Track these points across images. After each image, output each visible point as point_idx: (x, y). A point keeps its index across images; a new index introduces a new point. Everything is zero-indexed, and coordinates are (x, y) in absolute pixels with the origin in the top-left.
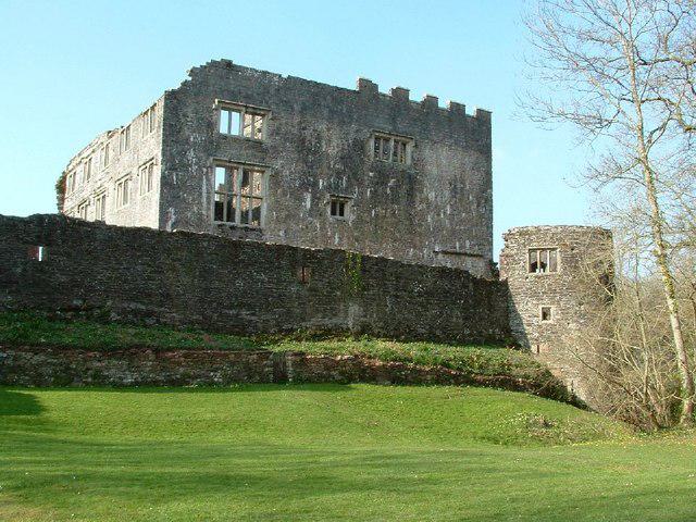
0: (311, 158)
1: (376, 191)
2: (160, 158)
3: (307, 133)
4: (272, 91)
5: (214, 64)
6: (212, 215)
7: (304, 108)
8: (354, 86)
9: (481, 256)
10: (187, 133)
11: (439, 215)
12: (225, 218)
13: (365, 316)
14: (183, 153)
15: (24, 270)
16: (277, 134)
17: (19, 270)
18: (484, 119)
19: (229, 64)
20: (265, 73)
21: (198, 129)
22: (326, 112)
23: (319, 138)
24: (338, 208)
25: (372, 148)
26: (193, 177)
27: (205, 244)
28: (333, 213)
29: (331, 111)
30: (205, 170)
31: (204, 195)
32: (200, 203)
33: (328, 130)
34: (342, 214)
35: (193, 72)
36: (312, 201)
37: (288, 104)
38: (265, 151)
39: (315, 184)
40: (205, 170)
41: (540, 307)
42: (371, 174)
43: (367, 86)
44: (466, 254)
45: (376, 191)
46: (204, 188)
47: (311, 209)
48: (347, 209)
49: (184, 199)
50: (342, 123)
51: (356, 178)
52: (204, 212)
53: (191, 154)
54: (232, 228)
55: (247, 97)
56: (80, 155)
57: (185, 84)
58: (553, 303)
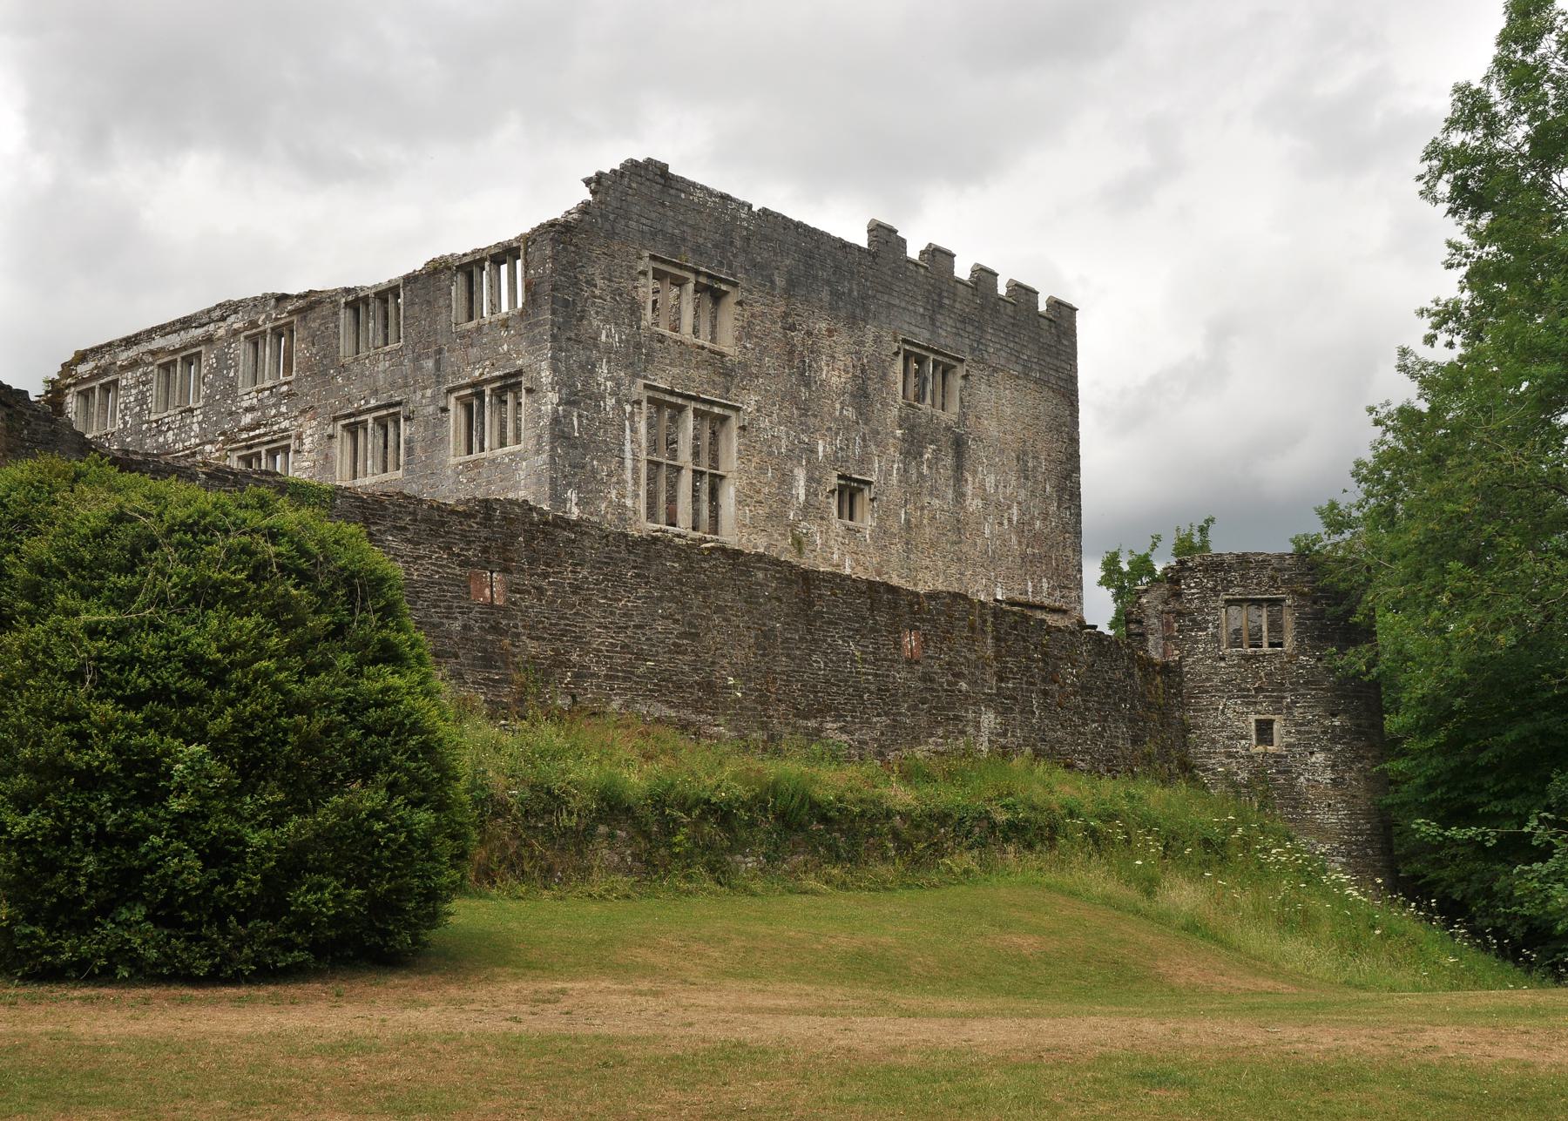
2: (546, 377)
6: (642, 507)
7: (792, 284)
8: (862, 240)
9: (1065, 612)
11: (1001, 524)
12: (663, 518)
13: (1004, 735)
14: (589, 368)
15: (465, 627)
16: (749, 336)
17: (457, 626)
18: (1063, 315)
19: (663, 168)
20: (725, 198)
21: (613, 318)
22: (825, 295)
24: (850, 492)
25: (900, 377)
30: (628, 408)
31: (629, 463)
33: (830, 332)
36: (810, 479)
37: (761, 270)
38: (728, 374)
39: (813, 451)
40: (628, 408)
41: (1252, 718)
43: (884, 236)
46: (628, 447)
49: (594, 471)
50: (853, 321)
52: (629, 503)
53: (603, 370)
57: (584, 209)
58: (1277, 711)
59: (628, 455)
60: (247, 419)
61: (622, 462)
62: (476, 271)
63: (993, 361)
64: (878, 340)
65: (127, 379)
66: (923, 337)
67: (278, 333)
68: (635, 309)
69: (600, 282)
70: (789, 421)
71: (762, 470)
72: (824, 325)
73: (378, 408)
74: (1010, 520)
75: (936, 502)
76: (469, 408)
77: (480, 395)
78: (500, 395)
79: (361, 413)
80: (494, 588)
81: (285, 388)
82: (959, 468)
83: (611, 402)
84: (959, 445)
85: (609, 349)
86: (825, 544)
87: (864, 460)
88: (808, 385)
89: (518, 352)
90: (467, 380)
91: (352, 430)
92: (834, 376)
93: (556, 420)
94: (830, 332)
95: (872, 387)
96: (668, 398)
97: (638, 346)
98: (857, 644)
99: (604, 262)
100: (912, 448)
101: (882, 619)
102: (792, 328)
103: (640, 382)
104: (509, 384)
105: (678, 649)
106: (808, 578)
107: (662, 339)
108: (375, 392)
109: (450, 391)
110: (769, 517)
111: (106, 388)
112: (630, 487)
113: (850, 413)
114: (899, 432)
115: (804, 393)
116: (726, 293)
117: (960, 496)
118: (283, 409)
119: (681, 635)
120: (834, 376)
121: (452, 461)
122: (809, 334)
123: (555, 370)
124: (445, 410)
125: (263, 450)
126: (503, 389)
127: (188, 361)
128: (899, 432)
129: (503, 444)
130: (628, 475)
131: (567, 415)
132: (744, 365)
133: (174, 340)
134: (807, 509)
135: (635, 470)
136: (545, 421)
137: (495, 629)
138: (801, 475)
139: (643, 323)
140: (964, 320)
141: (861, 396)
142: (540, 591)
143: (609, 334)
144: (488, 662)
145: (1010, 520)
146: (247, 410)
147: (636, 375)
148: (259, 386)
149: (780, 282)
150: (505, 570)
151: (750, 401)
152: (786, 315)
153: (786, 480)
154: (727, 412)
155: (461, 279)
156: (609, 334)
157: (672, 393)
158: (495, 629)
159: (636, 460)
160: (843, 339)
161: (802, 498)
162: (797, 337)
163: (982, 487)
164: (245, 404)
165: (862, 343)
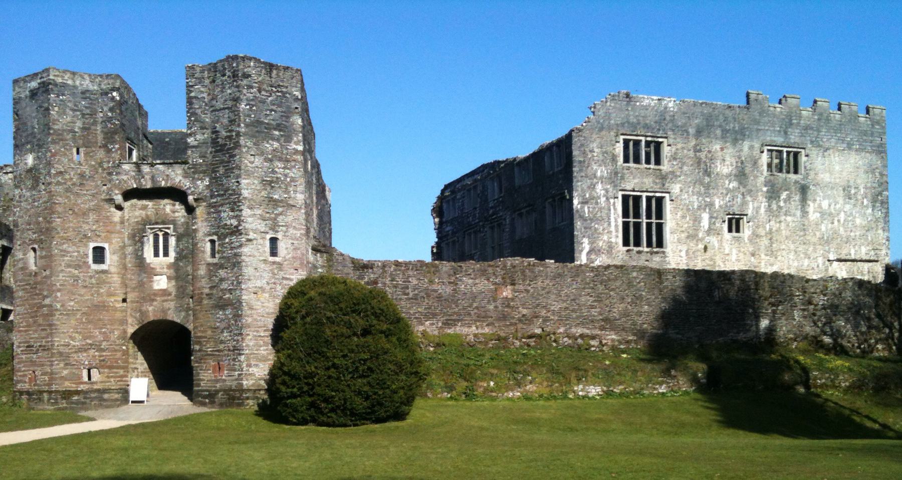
4: (668, 118)
11: (833, 223)
14: (592, 187)
15: (496, 307)
16: (675, 159)
17: (491, 307)
21: (603, 163)
26: (601, 209)
27: (635, 274)
28: (730, 230)
31: (613, 224)
32: (610, 232)
34: (738, 231)
36: (711, 217)
39: (711, 205)
44: (861, 261)
47: (710, 229)
49: (596, 229)
50: (735, 141)
53: (599, 187)
54: (639, 252)
55: (647, 127)
59: (612, 220)
61: (609, 224)
63: (827, 145)
64: (751, 148)
68: (614, 158)
69: (596, 150)
70: (699, 194)
71: (684, 217)
72: (718, 147)
74: (839, 221)
75: (789, 219)
80: (507, 292)
82: (804, 201)
83: (603, 199)
84: (804, 190)
85: (602, 177)
87: (744, 203)
88: (709, 176)
92: (725, 167)
94: (722, 149)
95: (748, 170)
97: (616, 173)
100: (773, 194)
102: (700, 151)
105: (592, 307)
110: (688, 237)
112: (614, 233)
113: (734, 184)
114: (765, 189)
115: (707, 179)
117: (805, 213)
119: (595, 301)
120: (725, 167)
122: (709, 152)
128: (765, 189)
130: (613, 228)
131: (582, 208)
132: (673, 173)
134: (709, 232)
135: (616, 226)
137: (508, 306)
138: (705, 217)
139: (619, 164)
140: (807, 128)
141: (741, 175)
142: (528, 291)
144: (504, 317)
145: (839, 221)
149: (692, 131)
151: (676, 188)
152: (696, 145)
153: (697, 220)
154: (663, 195)
157: (634, 191)
158: (508, 306)
159: (616, 221)
160: (730, 151)
161: (707, 227)
162: (703, 155)
163: (820, 206)
165: (741, 150)
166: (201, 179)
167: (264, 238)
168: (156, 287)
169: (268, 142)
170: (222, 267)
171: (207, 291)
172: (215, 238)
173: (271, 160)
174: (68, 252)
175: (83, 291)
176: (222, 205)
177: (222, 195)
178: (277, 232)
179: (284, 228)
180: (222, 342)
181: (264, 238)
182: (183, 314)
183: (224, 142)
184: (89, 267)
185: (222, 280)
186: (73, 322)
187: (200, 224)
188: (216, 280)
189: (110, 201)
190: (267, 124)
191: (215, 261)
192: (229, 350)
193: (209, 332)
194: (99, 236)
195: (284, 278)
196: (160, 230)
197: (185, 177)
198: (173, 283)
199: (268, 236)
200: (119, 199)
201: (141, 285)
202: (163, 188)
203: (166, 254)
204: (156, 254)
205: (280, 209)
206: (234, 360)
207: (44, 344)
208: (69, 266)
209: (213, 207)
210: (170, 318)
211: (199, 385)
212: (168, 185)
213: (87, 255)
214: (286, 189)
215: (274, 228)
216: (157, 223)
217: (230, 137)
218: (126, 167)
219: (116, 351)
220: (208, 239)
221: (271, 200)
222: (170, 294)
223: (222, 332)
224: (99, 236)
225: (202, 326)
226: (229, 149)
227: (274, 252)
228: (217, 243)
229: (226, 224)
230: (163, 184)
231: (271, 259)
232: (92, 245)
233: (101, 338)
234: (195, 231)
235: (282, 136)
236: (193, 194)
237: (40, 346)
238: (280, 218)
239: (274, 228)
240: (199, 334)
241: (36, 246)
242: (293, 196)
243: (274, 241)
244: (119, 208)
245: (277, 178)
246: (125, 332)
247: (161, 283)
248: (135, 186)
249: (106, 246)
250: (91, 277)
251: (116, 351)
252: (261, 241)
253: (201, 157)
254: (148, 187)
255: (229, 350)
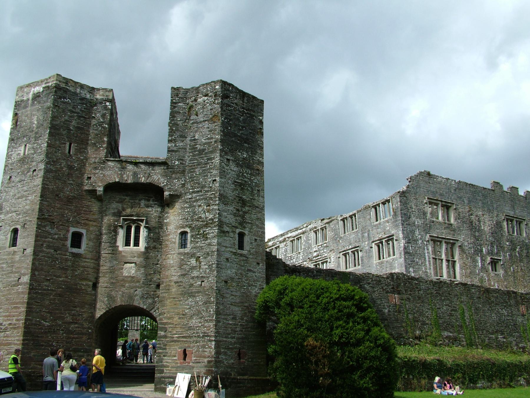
0: (477, 234)
1: (511, 254)
2: (401, 236)
3: (473, 217)
5: (421, 173)
7: (470, 202)
10: (414, 219)
14: (413, 232)
15: (389, 311)
17: (386, 311)
23: (479, 221)
25: (506, 226)
29: (483, 203)
30: (425, 243)
31: (427, 259)
33: (483, 215)
34: (496, 271)
35: (411, 179)
38: (454, 230)
39: (481, 251)
40: (425, 243)
42: (507, 243)
45: (511, 254)
46: (426, 255)
48: (498, 267)
50: (489, 211)
51: (501, 248)
52: (428, 271)
53: (417, 233)
55: (441, 195)
56: (282, 235)
59: (427, 257)
60: (315, 254)
62: (378, 207)
65: (282, 245)
66: (512, 213)
67: (322, 229)
68: (425, 214)
69: (414, 207)
72: (481, 213)
73: (352, 249)
76: (379, 246)
77: (382, 243)
78: (387, 241)
79: (347, 250)
81: (325, 245)
83: (420, 241)
86: (489, 280)
89: (392, 229)
90: (377, 239)
91: (345, 255)
93: (405, 248)
96: (437, 239)
97: (427, 225)
98: (505, 310)
99: (415, 201)
101: (512, 302)
102: (472, 215)
103: (428, 235)
104: (390, 238)
105: (451, 315)
106: (488, 291)
107: (433, 222)
108: (351, 244)
109: (373, 242)
111: (276, 248)
116: (451, 206)
118: (325, 251)
119: (452, 310)
121: (375, 262)
123: (403, 233)
124: (371, 248)
125: (320, 262)
126: (388, 240)
127: (298, 239)
129: (389, 256)
130: (427, 263)
133: (294, 234)
135: (429, 261)
136: (402, 249)
138: (479, 259)
139: (427, 218)
143: (418, 222)
146: (315, 251)
147: (427, 233)
148: (318, 245)
149: (466, 201)
150: (399, 293)
153: (475, 261)
155: (373, 209)
156: (418, 222)
161: (480, 266)
164: (314, 250)
166: (178, 179)
167: (234, 232)
168: (125, 274)
169: (239, 152)
170: (193, 255)
171: (175, 278)
172: (188, 230)
173: (242, 167)
174: (50, 234)
175: (59, 273)
176: (197, 201)
177: (198, 192)
178: (245, 227)
179: (250, 225)
180: (190, 328)
181: (234, 232)
182: (150, 301)
183: (202, 147)
184: (67, 250)
185: (193, 268)
186: (47, 302)
187: (172, 218)
188: (187, 267)
189: (92, 192)
190: (240, 137)
191: (187, 250)
192: (199, 336)
193: (176, 318)
194: (78, 223)
195: (250, 270)
196: (134, 221)
197: (163, 176)
198: (142, 270)
199: (238, 231)
200: (100, 189)
201: (112, 270)
202: (143, 184)
203: (137, 244)
204: (127, 244)
205: (247, 208)
206: (204, 347)
207: (14, 322)
208: (49, 247)
209: (187, 202)
210: (136, 303)
211: (162, 372)
212: (148, 181)
213: (66, 239)
214: (252, 191)
215: (242, 224)
216: (132, 216)
217: (209, 144)
218: (110, 163)
219: (83, 334)
220: (179, 231)
221: (241, 199)
222: (138, 282)
223: (191, 317)
224: (78, 223)
225: (168, 312)
226: (206, 153)
227: (241, 247)
228: (189, 235)
229: (200, 217)
230: (143, 180)
231: (240, 251)
232: (72, 230)
233: (69, 319)
234: (167, 224)
235: (250, 148)
236: (170, 190)
237: (10, 324)
238: (247, 216)
239: (242, 224)
240: (165, 321)
241: (19, 227)
242: (256, 198)
243: (241, 236)
244: (99, 199)
245: (246, 181)
246: (93, 316)
247: (130, 270)
248: (117, 180)
249: (84, 231)
250: (67, 260)
251: (83, 334)
252: (231, 234)
253: (178, 160)
254: (129, 182)
255: (199, 336)
